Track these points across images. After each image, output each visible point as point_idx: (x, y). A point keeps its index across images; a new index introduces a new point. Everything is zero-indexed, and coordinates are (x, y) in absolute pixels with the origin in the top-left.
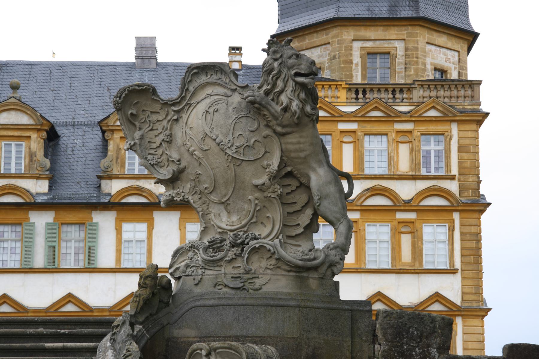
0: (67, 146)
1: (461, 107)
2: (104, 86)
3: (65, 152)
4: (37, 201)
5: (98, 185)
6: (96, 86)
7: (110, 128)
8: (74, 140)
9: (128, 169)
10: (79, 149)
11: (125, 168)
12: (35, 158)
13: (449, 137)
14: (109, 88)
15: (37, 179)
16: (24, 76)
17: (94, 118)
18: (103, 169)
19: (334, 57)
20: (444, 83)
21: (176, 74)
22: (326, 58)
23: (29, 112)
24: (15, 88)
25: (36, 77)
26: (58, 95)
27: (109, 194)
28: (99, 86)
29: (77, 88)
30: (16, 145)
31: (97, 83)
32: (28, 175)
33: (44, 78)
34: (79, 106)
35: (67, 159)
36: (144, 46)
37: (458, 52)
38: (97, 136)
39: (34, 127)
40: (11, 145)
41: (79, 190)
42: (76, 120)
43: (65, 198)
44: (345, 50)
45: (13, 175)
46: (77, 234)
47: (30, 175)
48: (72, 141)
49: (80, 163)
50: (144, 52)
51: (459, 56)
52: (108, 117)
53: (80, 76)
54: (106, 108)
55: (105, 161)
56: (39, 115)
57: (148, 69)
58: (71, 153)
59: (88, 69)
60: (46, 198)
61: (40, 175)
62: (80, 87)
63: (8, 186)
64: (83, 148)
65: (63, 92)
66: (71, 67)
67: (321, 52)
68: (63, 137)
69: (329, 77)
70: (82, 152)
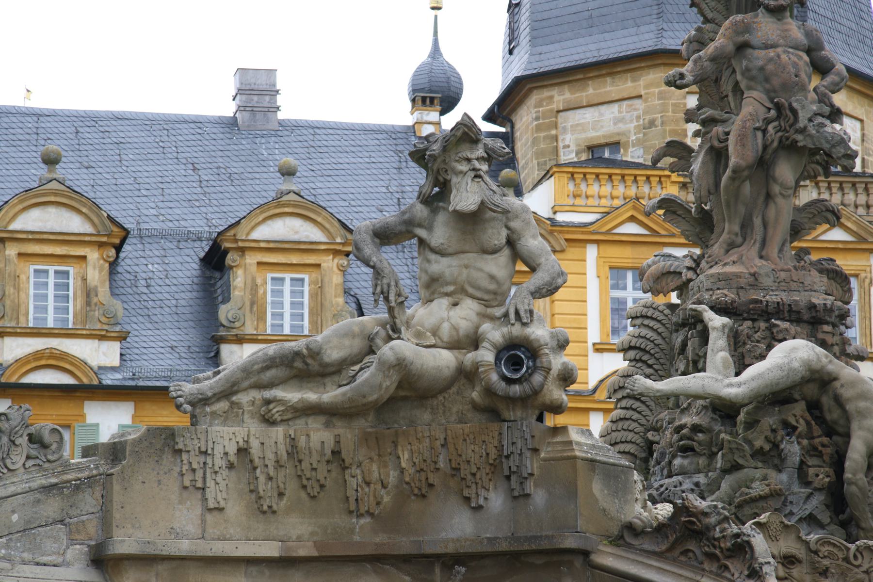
0: (136, 277)
2: (184, 161)
3: (134, 289)
4: (104, 382)
5: (212, 354)
6: (170, 161)
7: (240, 244)
8: (146, 265)
9: (272, 325)
10: (160, 282)
11: (265, 322)
12: (95, 300)
14: (196, 165)
15: (99, 340)
16: (27, 137)
17: (176, 223)
18: (225, 322)
19: (652, 123)
20: (857, 180)
21: (319, 143)
22: (633, 125)
23: (84, 210)
24: (51, 161)
25: (49, 139)
26: (99, 176)
28: (176, 160)
29: (133, 163)
30: (56, 272)
31: (170, 156)
32: (84, 332)
33: (66, 142)
34: (144, 199)
35: (140, 301)
36: (256, 87)
37: (861, 121)
38: (189, 259)
39: (94, 239)
40: (47, 272)
41: (179, 362)
42: (143, 226)
43: (156, 377)
44: (673, 112)
45: (57, 331)
47: (88, 332)
48: (144, 268)
49: (167, 309)
50: (255, 98)
51: (863, 129)
52: (238, 223)
53: (136, 140)
54: (197, 204)
55: (229, 307)
56: (106, 215)
57: (265, 132)
58: (145, 290)
59: (148, 128)
60: (118, 376)
61: (107, 331)
62: (140, 163)
63: (47, 351)
64: (167, 281)
65: (107, 170)
66: (114, 123)
67: (620, 112)
68: (125, 258)
69: (641, 161)
70: (167, 289)
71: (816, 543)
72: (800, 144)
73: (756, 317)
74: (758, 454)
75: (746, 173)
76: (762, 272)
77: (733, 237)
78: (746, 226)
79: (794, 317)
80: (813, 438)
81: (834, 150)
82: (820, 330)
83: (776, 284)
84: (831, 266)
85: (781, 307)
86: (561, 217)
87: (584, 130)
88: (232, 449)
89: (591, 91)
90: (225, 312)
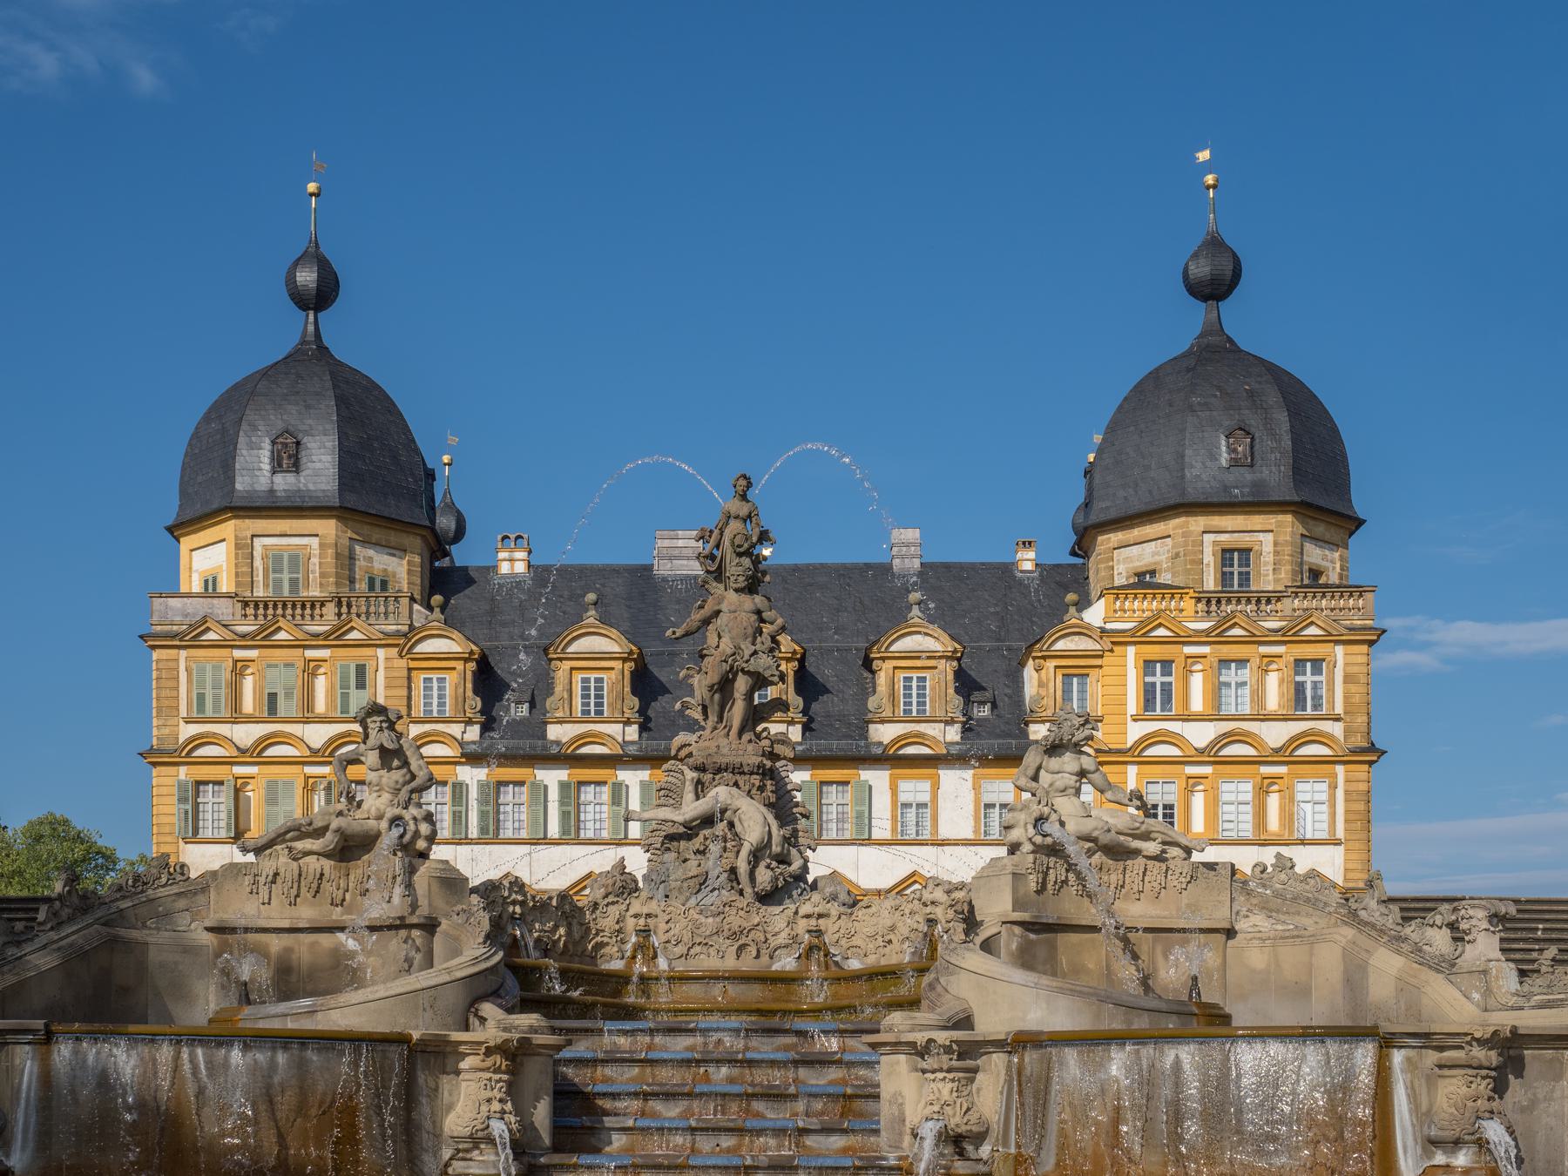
1: (1348, 622)
13: (1332, 663)
27: (880, 743)
46: (840, 795)
50: (904, 549)
74: (698, 852)
76: (721, 745)
79: (736, 771)
86: (1109, 626)
87: (1132, 562)
88: (271, 874)
89: (1136, 533)
90: (872, 703)
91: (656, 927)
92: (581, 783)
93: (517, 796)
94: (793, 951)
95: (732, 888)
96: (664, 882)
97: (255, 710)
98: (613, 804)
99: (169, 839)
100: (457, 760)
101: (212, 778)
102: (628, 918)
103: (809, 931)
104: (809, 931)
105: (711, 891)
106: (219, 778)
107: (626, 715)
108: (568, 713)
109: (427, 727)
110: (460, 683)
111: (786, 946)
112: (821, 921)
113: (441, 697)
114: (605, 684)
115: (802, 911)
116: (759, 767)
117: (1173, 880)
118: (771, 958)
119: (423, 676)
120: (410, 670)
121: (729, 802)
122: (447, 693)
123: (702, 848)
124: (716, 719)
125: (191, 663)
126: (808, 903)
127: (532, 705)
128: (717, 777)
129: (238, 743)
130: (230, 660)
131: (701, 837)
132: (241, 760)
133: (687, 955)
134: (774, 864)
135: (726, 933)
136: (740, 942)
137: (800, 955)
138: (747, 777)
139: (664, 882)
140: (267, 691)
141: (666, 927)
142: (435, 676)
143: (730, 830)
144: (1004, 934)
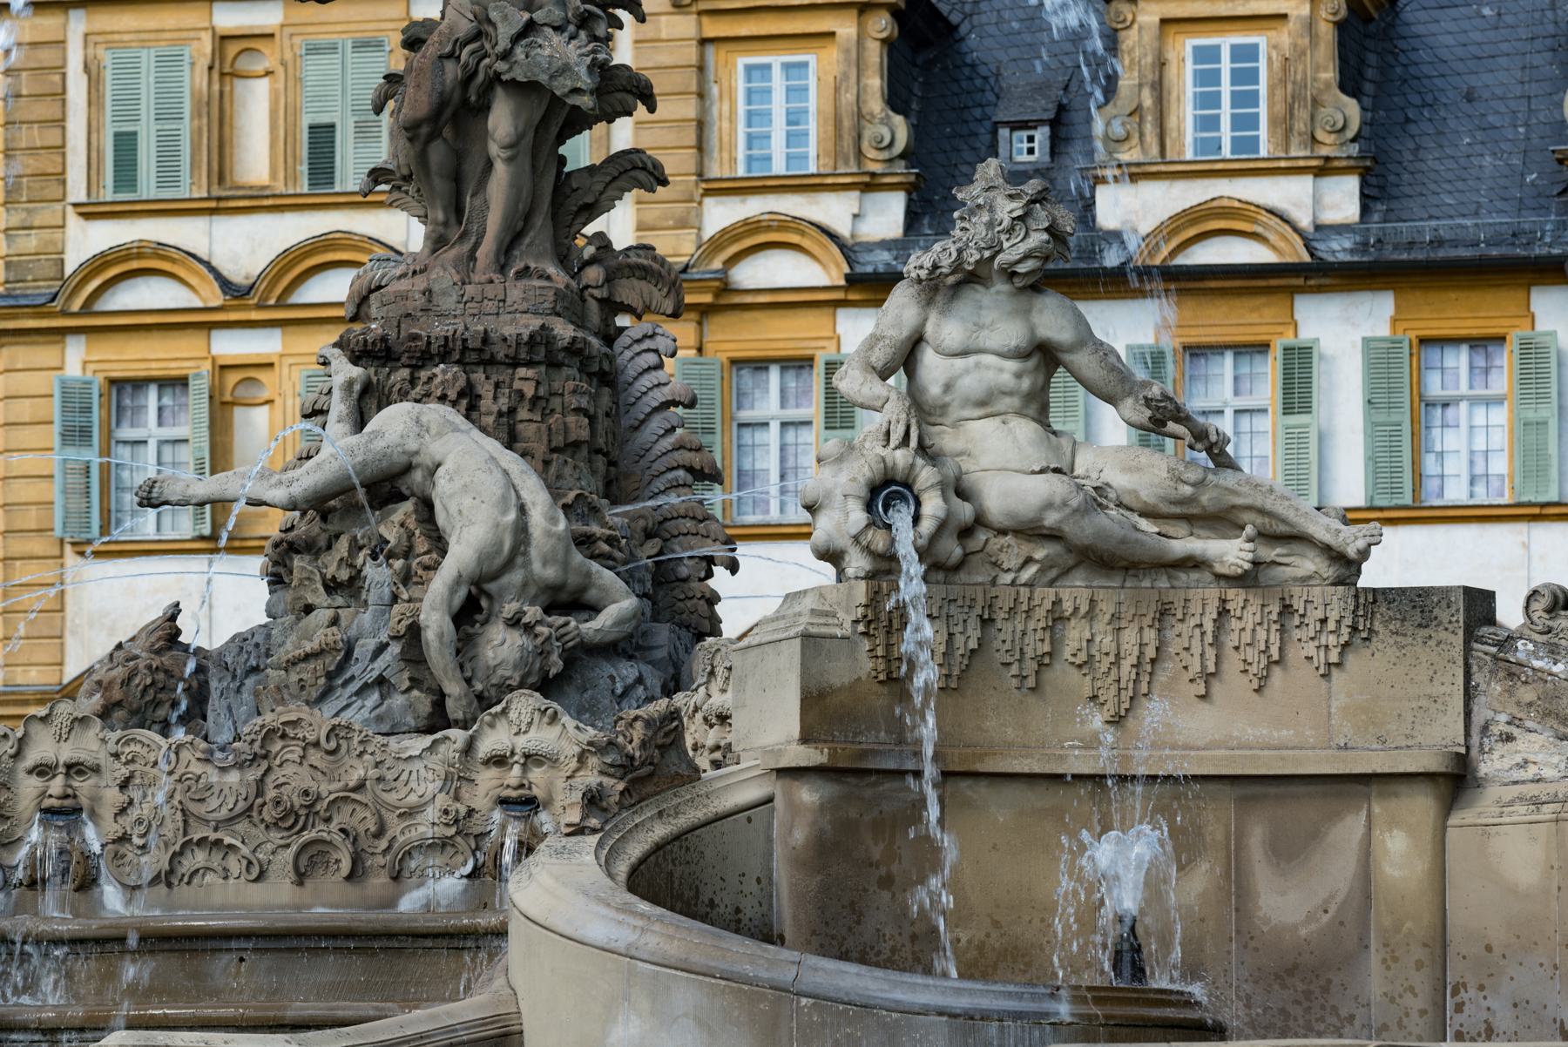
71: (117, 743)
72: (504, 78)
73: (414, 362)
74: (332, 586)
75: (424, 130)
76: (436, 288)
77: (441, 229)
78: (458, 210)
79: (473, 357)
80: (418, 556)
81: (556, 83)
82: (517, 376)
83: (462, 306)
84: (640, 260)
85: (451, 345)
91: (95, 799)
92: (1196, 351)
93: (1246, 385)
94: (460, 858)
95: (415, 683)
96: (255, 670)
97: (273, 174)
98: (1288, 409)
99: (37, 546)
100: (840, 295)
101: (156, 370)
102: (22, 775)
103: (504, 802)
104: (504, 802)
105: (359, 693)
106: (174, 369)
107: (1324, 151)
108: (1154, 151)
109: (754, 207)
110: (846, 76)
111: (443, 844)
112: (537, 775)
113: (794, 118)
114: (1262, 65)
115: (485, 747)
116: (532, 341)
117: (1303, 647)
118: (396, 878)
119: (742, 61)
120: (703, 42)
121: (412, 445)
122: (812, 104)
123: (344, 575)
124: (440, 216)
125: (100, 51)
126: (502, 725)
127: (1057, 144)
128: (424, 374)
129: (228, 270)
130: (207, 38)
131: (342, 547)
132: (233, 316)
133: (171, 872)
134: (533, 612)
135: (269, 814)
136: (307, 836)
137: (475, 868)
138: (503, 375)
139: (255, 670)
140: (306, 121)
141: (122, 799)
142: (776, 60)
143: (420, 521)
144: (779, 803)
